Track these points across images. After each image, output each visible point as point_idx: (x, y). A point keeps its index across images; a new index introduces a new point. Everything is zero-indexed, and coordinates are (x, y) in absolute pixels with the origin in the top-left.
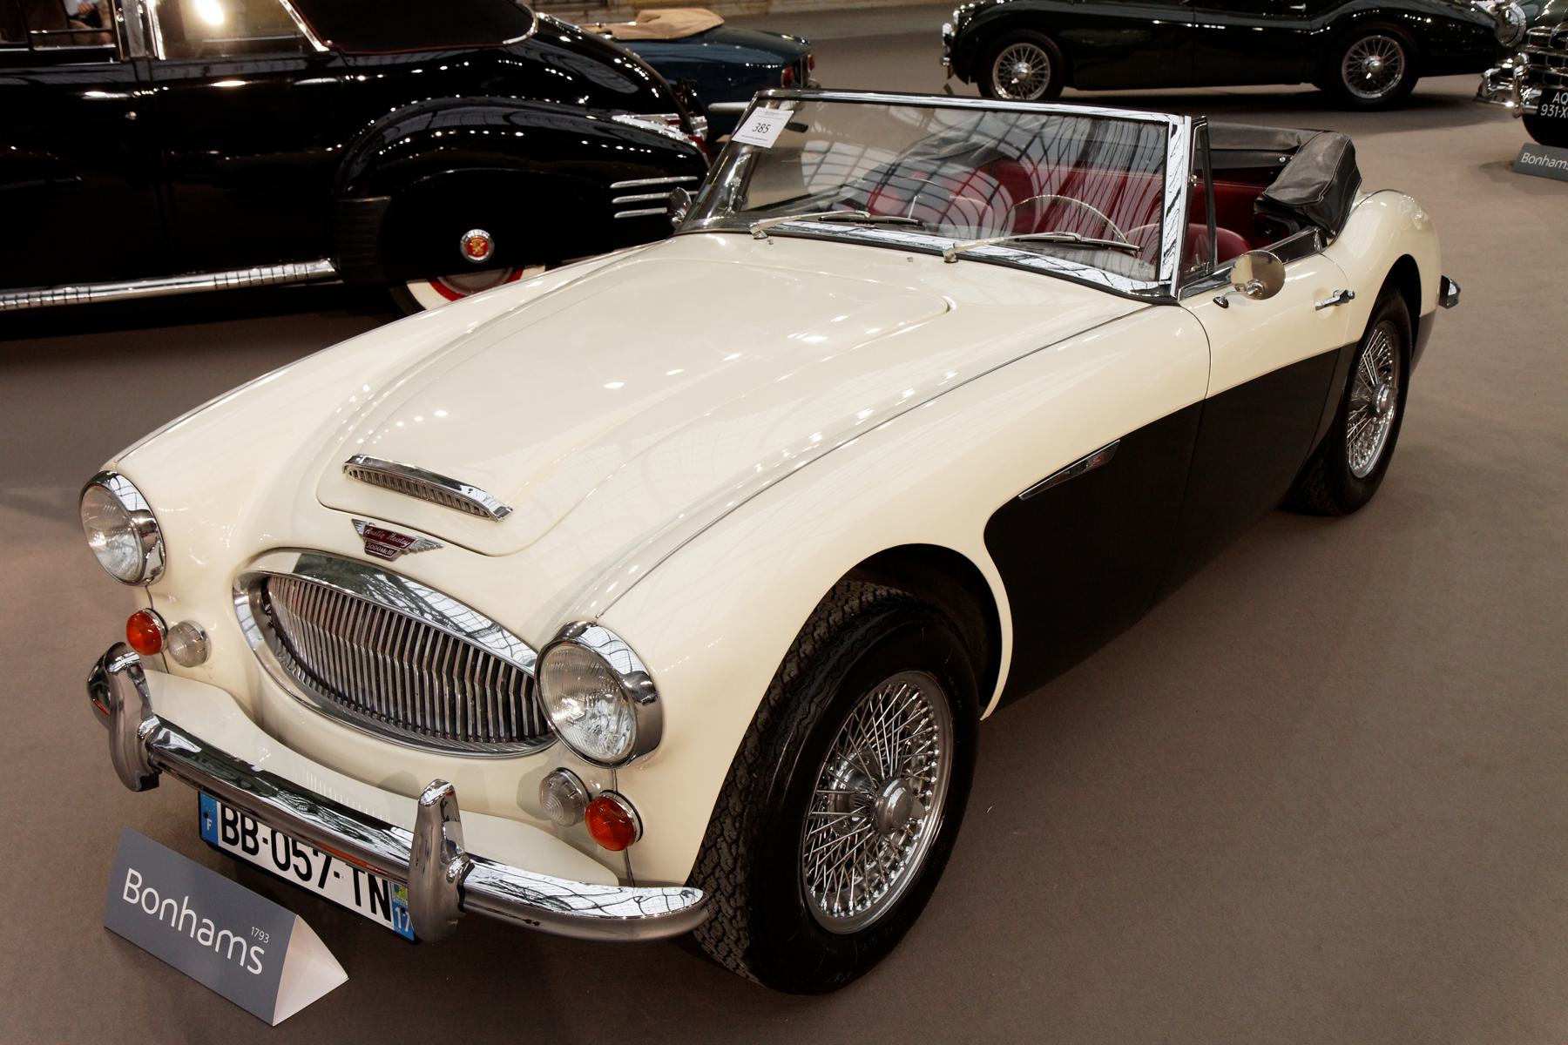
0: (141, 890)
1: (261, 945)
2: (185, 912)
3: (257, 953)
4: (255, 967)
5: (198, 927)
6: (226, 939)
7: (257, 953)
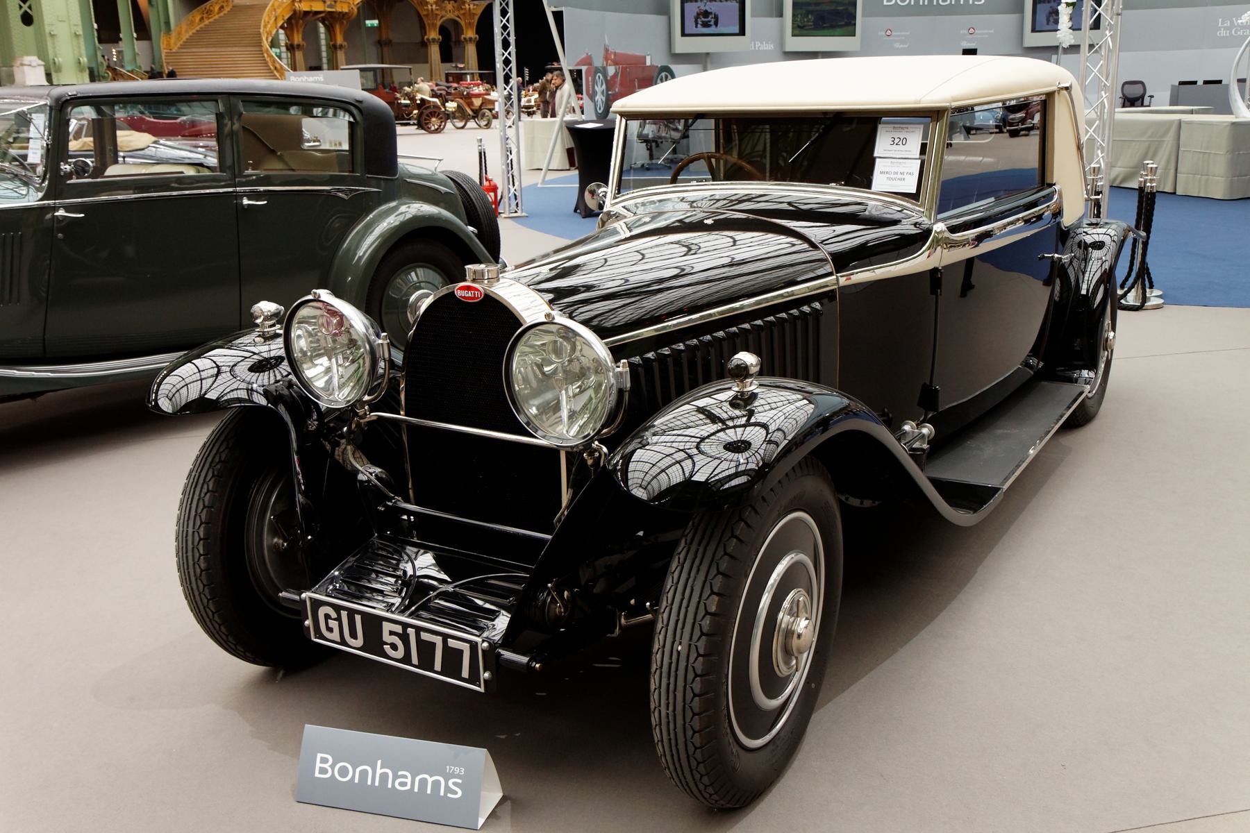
0: (333, 767)
1: (458, 776)
2: (379, 771)
3: (454, 784)
4: (456, 793)
5: (395, 777)
6: (423, 782)
7: (454, 784)
